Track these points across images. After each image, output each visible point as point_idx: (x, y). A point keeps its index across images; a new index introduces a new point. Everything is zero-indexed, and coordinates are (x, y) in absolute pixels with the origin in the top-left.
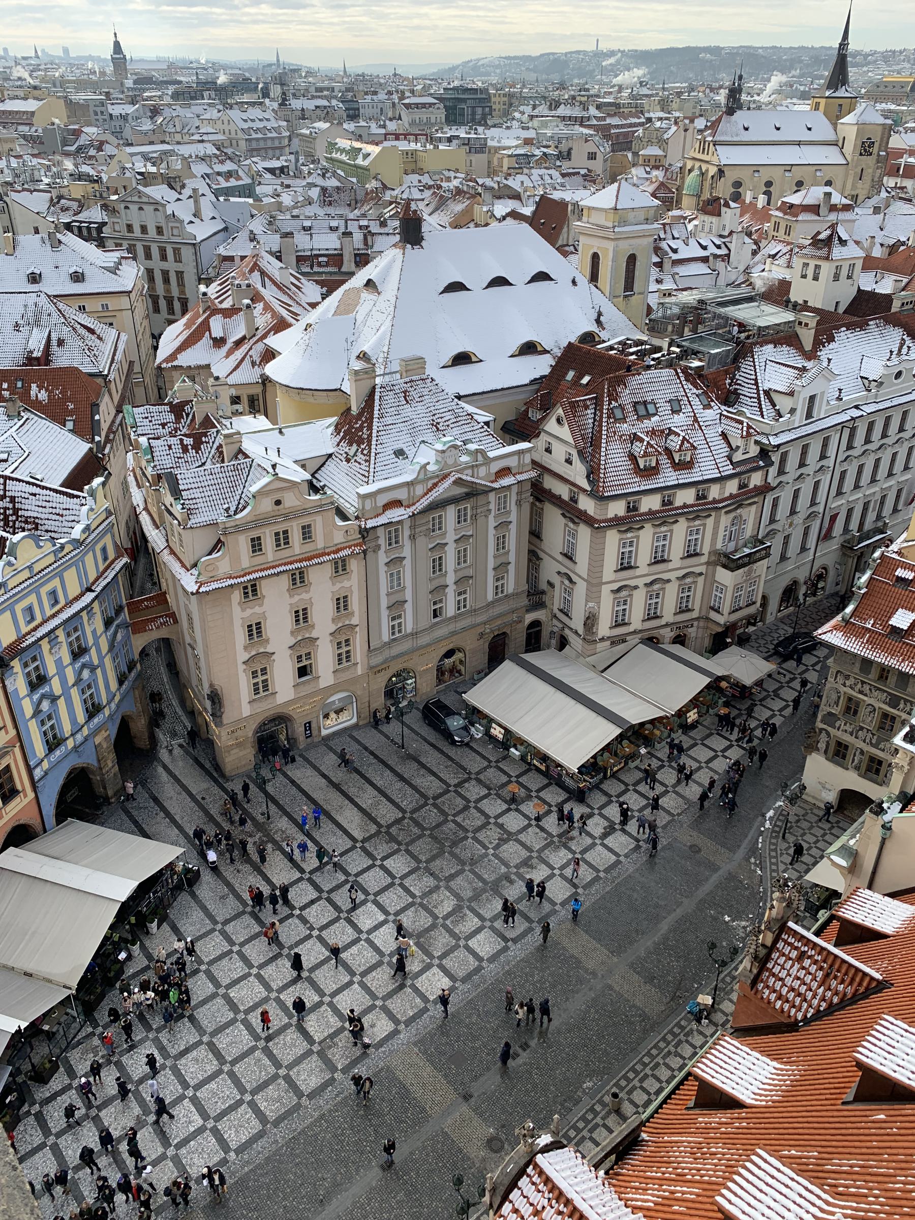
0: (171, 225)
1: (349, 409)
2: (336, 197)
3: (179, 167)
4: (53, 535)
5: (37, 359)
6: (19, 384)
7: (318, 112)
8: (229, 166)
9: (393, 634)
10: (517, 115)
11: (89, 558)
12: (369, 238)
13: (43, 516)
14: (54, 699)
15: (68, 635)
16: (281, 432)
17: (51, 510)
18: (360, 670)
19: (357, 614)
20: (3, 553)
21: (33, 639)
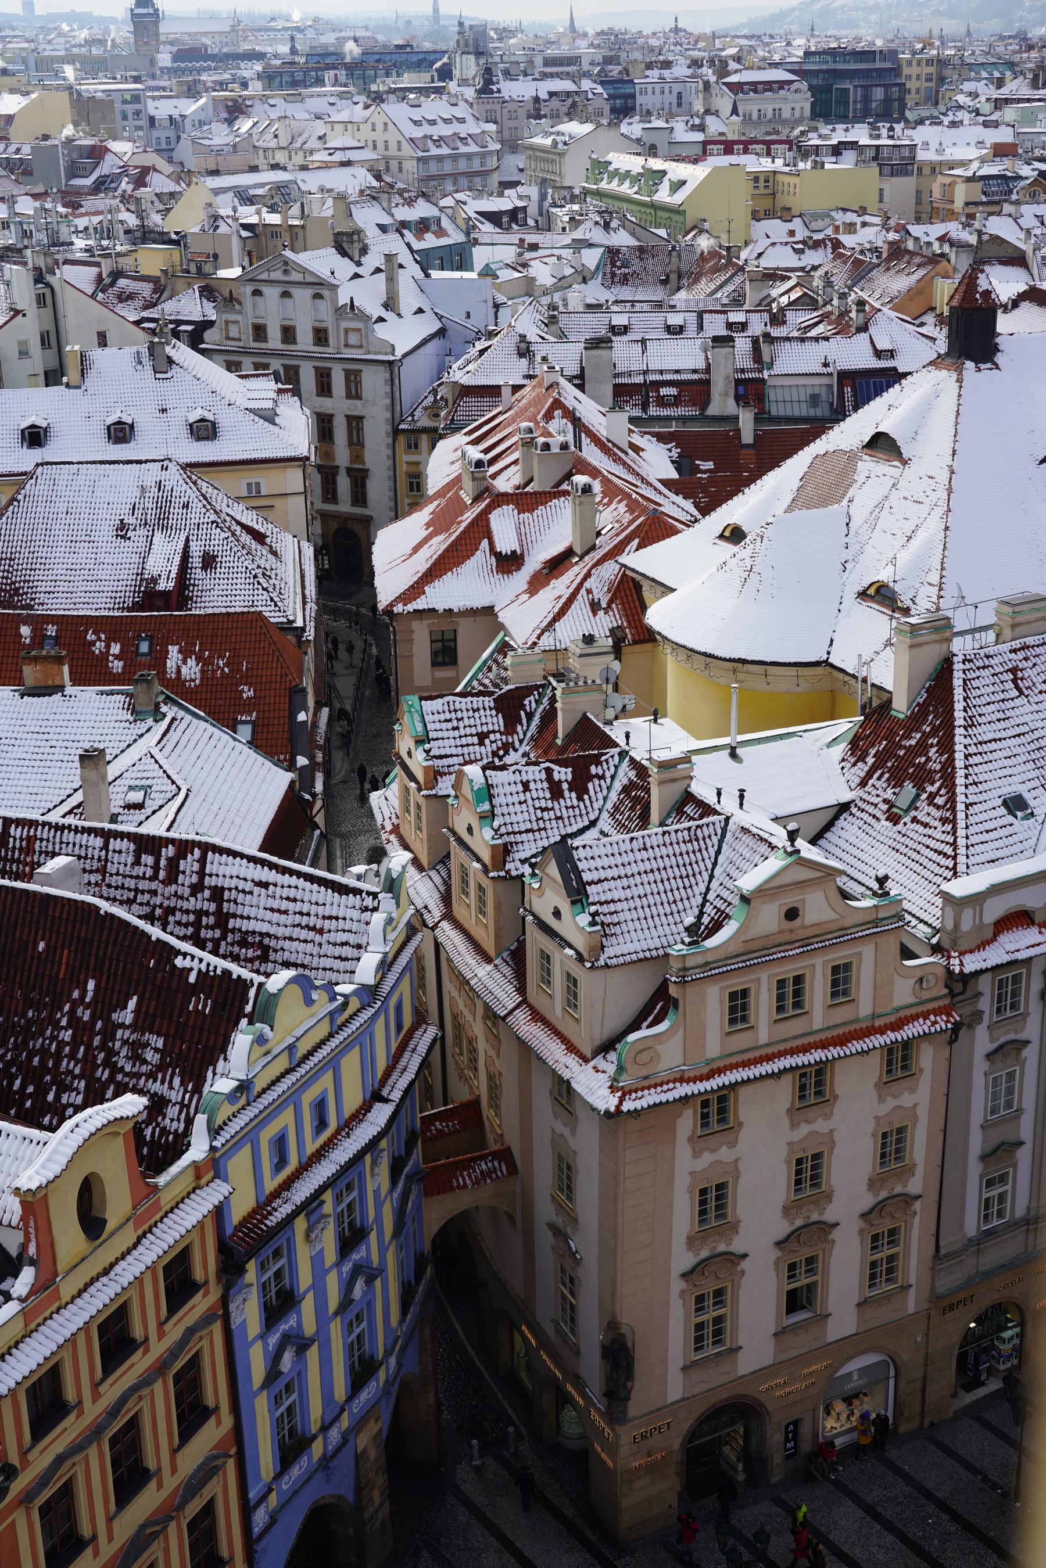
0: (344, 324)
1: (887, 705)
2: (636, 266)
3: (329, 213)
5: (165, 594)
6: (144, 647)
7: (555, 103)
8: (422, 210)
10: (961, 99)
11: (379, 1027)
12: (765, 348)
13: (281, 931)
15: (338, 1199)
16: (733, 755)
18: (912, 1303)
19: (920, 1171)
20: (241, 1014)
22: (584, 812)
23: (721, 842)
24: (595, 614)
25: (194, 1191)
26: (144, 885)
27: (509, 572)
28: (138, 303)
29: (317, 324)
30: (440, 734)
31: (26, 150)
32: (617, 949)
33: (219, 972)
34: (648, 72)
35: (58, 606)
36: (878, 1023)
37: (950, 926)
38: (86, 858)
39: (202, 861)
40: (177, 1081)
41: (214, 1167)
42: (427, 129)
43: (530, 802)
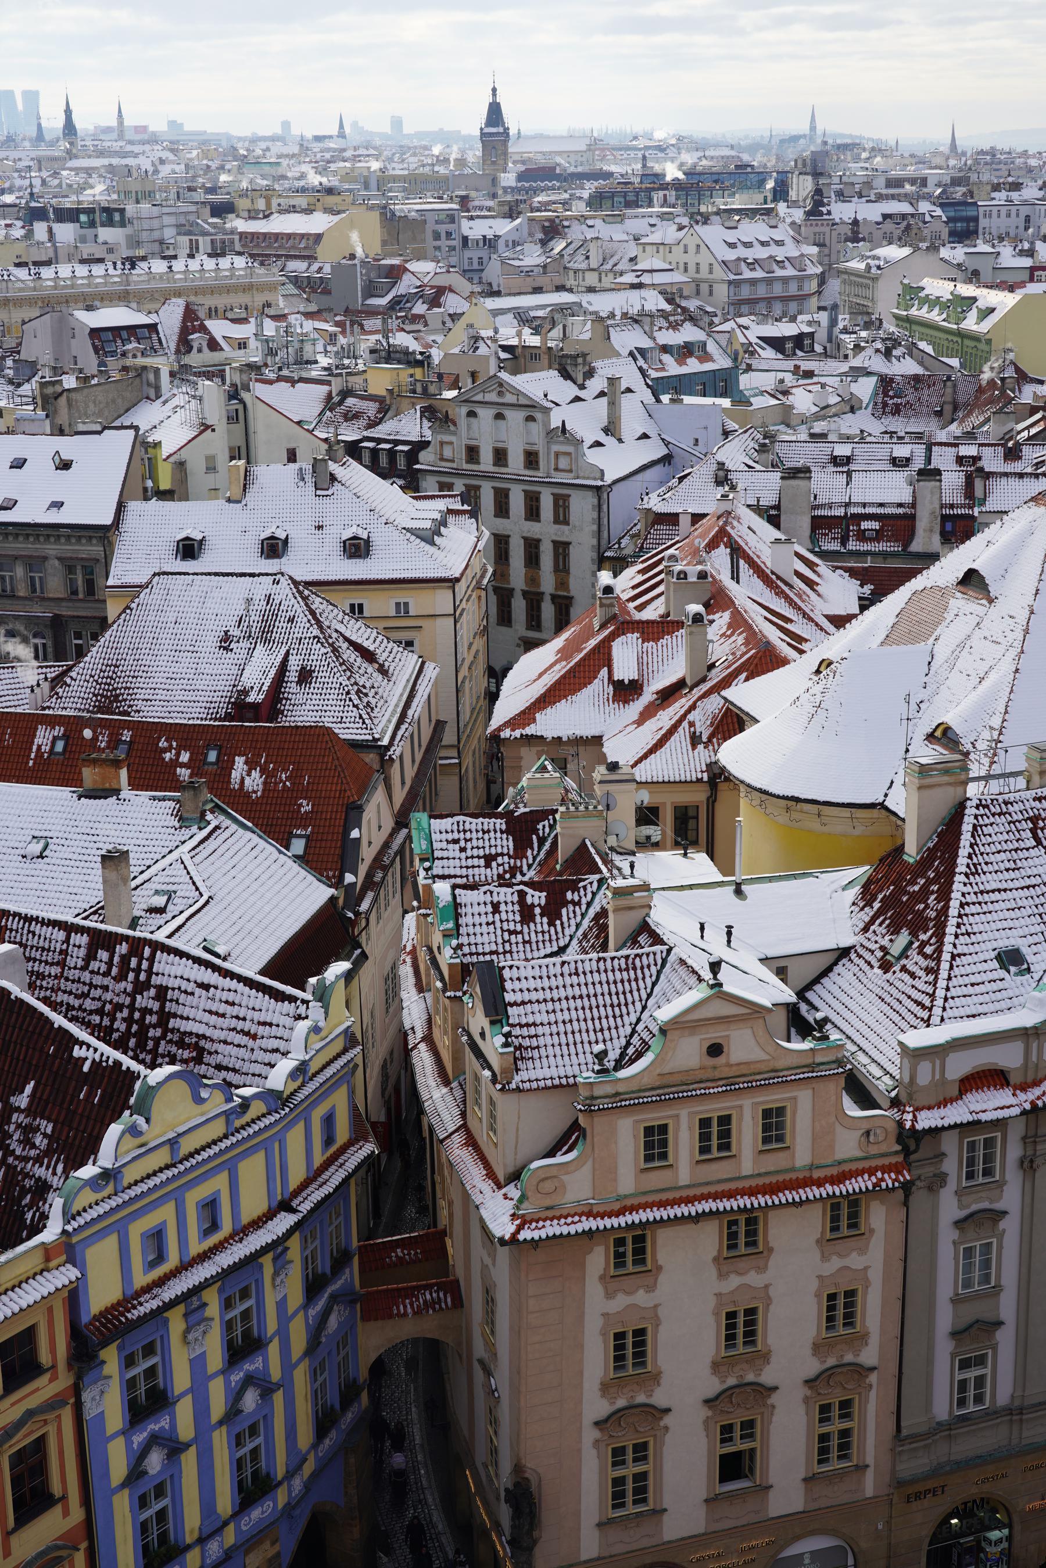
0: (555, 448)
1: (900, 849)
3: (587, 336)
4: (230, 1077)
5: (254, 706)
6: (212, 756)
7: (889, 226)
8: (689, 333)
9: (962, 1402)
11: (295, 1138)
12: (978, 484)
13: (217, 1034)
14: (175, 1449)
15: (227, 1304)
16: (739, 892)
17: (234, 1023)
18: (870, 1485)
19: (874, 1340)
21: (154, 1304)
22: (554, 937)
23: (659, 973)
24: (694, 746)
25: (41, 1273)
26: (98, 980)
27: (626, 702)
28: (362, 422)
29: (528, 447)
30: (445, 854)
31: (327, 269)
32: (530, 1073)
33: (110, 1063)
34: (993, 195)
35: (152, 713)
36: (817, 1174)
37: (907, 1079)
38: (49, 950)
39: (152, 960)
40: (60, 1168)
41: (68, 1249)
42: (741, 252)
43: (498, 924)
